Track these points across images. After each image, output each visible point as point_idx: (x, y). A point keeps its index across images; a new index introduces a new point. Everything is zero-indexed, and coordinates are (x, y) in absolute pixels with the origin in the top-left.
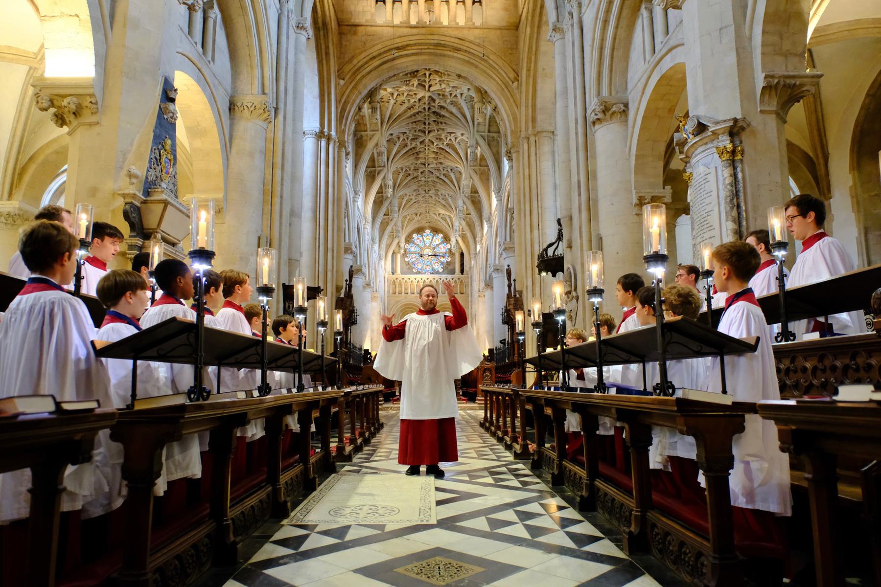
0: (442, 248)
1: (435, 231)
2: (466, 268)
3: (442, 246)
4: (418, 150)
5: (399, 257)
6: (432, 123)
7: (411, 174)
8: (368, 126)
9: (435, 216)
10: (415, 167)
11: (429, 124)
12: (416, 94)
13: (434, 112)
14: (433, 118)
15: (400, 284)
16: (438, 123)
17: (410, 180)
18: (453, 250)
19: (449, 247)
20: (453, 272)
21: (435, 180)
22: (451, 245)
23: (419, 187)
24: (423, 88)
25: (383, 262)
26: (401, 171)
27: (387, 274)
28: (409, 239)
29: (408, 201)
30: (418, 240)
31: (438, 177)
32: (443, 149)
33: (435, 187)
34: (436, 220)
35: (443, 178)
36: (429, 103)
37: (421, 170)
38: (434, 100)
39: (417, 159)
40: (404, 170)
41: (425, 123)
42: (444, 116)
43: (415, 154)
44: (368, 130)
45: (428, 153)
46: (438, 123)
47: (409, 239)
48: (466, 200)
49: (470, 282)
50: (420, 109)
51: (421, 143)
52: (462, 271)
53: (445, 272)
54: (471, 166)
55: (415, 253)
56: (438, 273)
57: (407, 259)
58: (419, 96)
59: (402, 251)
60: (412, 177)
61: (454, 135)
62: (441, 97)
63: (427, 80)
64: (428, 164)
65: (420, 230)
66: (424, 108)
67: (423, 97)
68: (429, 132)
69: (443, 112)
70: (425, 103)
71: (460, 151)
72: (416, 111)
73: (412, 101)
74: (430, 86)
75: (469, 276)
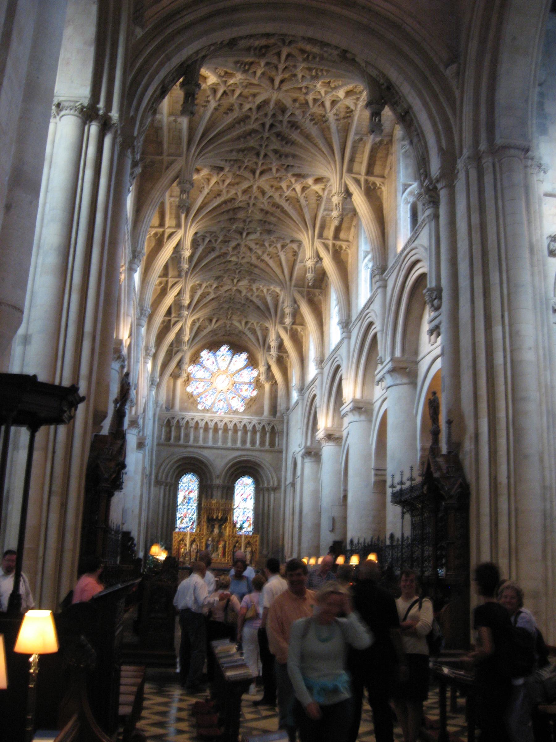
1: (236, 349)
3: (246, 372)
6: (271, 154)
8: (165, 146)
10: (225, 236)
15: (178, 427)
29: (203, 296)
34: (240, 332)
40: (207, 240)
43: (231, 212)
44: (165, 154)
45: (252, 211)
49: (285, 430)
51: (244, 192)
53: (247, 412)
56: (236, 412)
67: (266, 103)
71: (306, 211)
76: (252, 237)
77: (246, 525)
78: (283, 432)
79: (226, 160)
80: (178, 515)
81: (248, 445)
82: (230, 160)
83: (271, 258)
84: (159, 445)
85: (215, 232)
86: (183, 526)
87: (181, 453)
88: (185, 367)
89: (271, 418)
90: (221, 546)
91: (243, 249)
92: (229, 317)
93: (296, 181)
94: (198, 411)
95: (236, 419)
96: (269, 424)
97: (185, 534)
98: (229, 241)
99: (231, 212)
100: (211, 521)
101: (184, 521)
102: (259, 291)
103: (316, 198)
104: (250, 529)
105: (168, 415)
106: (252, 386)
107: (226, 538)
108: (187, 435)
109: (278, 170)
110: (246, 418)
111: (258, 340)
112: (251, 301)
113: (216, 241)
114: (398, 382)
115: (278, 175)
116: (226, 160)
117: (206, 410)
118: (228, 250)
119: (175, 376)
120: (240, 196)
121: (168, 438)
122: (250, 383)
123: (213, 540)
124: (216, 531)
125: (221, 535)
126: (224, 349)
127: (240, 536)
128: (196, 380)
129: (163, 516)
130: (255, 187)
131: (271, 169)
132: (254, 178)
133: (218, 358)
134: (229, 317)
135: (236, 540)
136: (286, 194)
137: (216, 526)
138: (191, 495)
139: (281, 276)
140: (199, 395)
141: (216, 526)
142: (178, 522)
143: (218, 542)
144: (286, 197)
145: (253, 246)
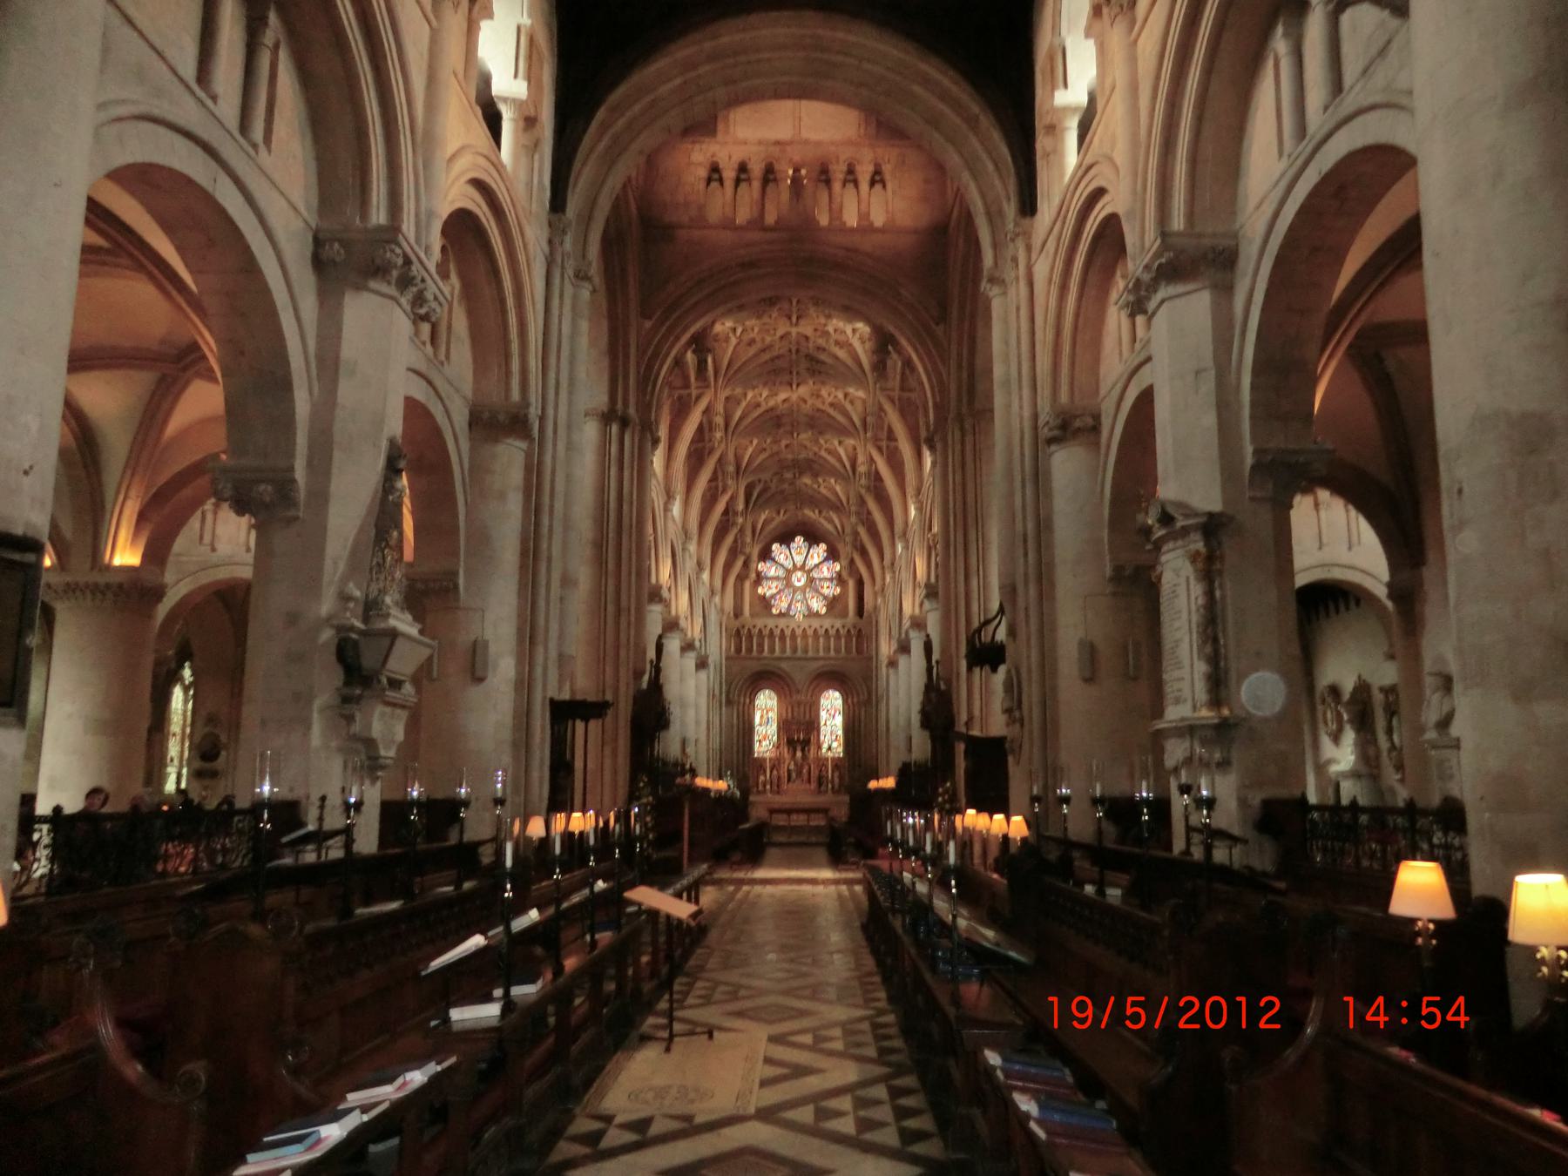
4: (778, 413)
5: (747, 585)
11: (798, 373)
12: (775, 329)
13: (807, 356)
14: (804, 364)
15: (750, 636)
16: (814, 371)
20: (844, 614)
24: (785, 319)
25: (717, 599)
27: (725, 618)
28: (766, 555)
30: (782, 556)
31: (815, 454)
32: (823, 411)
35: (823, 453)
36: (798, 343)
38: (807, 338)
39: (779, 426)
41: (791, 373)
42: (823, 363)
46: (814, 371)
47: (766, 555)
48: (863, 491)
49: (874, 633)
50: (781, 351)
52: (860, 611)
55: (777, 578)
56: (817, 615)
57: (760, 591)
58: (780, 332)
59: (753, 576)
62: (819, 333)
63: (794, 310)
65: (786, 539)
66: (790, 351)
68: (798, 385)
69: (823, 357)
70: (790, 343)
72: (775, 354)
73: (768, 339)
74: (798, 318)
75: (874, 623)
77: (835, 745)
78: (871, 635)
80: (756, 738)
81: (832, 653)
84: (727, 659)
86: (762, 749)
87: (754, 666)
88: (753, 566)
90: (805, 771)
94: (772, 615)
95: (816, 623)
97: (765, 760)
100: (791, 743)
101: (764, 743)
104: (841, 749)
105: (737, 624)
106: (835, 582)
107: (811, 761)
108: (761, 645)
110: (827, 623)
117: (781, 615)
119: (741, 579)
121: (738, 650)
122: (831, 580)
123: (796, 764)
124: (799, 754)
125: (804, 757)
126: (799, 540)
127: (827, 759)
128: (768, 579)
129: (738, 741)
133: (793, 551)
135: (822, 762)
137: (799, 748)
138: (770, 714)
139: (842, 470)
140: (773, 596)
141: (799, 748)
142: (757, 745)
143: (802, 767)
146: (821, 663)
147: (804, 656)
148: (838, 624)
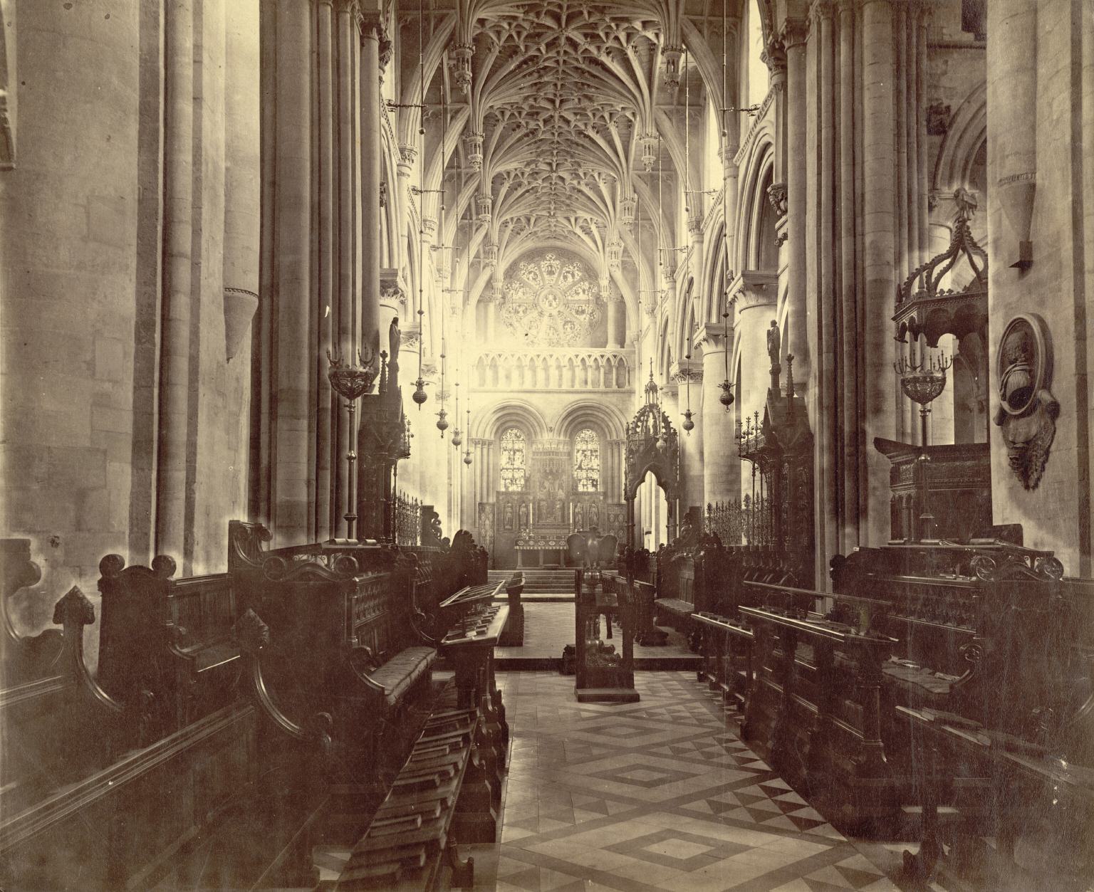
0: (580, 291)
2: (630, 334)
7: (523, 123)
9: (566, 223)
17: (519, 140)
18: (605, 294)
19: (595, 290)
21: (574, 138)
22: (599, 286)
23: (539, 156)
26: (500, 117)
29: (513, 189)
33: (572, 157)
37: (545, 115)
40: (507, 114)
54: (657, 104)
60: (524, 131)
61: (626, 25)
64: (562, 102)
76: (569, 105)
79: (518, 6)
82: (523, 6)
83: (597, 132)
85: (517, 103)
89: (618, 348)
91: (557, 122)
92: (552, 213)
93: (617, 26)
96: (615, 356)
98: (537, 113)
99: (536, 75)
102: (588, 176)
103: (648, 47)
109: (590, 13)
111: (595, 242)
112: (579, 191)
113: (520, 113)
114: (753, 303)
115: (592, 20)
116: (518, 6)
118: (538, 125)
120: (544, 52)
130: (563, 41)
131: (581, 13)
132: (560, 25)
134: (552, 213)
136: (607, 45)
144: (607, 48)
145: (570, 117)
146: (577, 397)
147: (557, 388)
148: (597, 352)
